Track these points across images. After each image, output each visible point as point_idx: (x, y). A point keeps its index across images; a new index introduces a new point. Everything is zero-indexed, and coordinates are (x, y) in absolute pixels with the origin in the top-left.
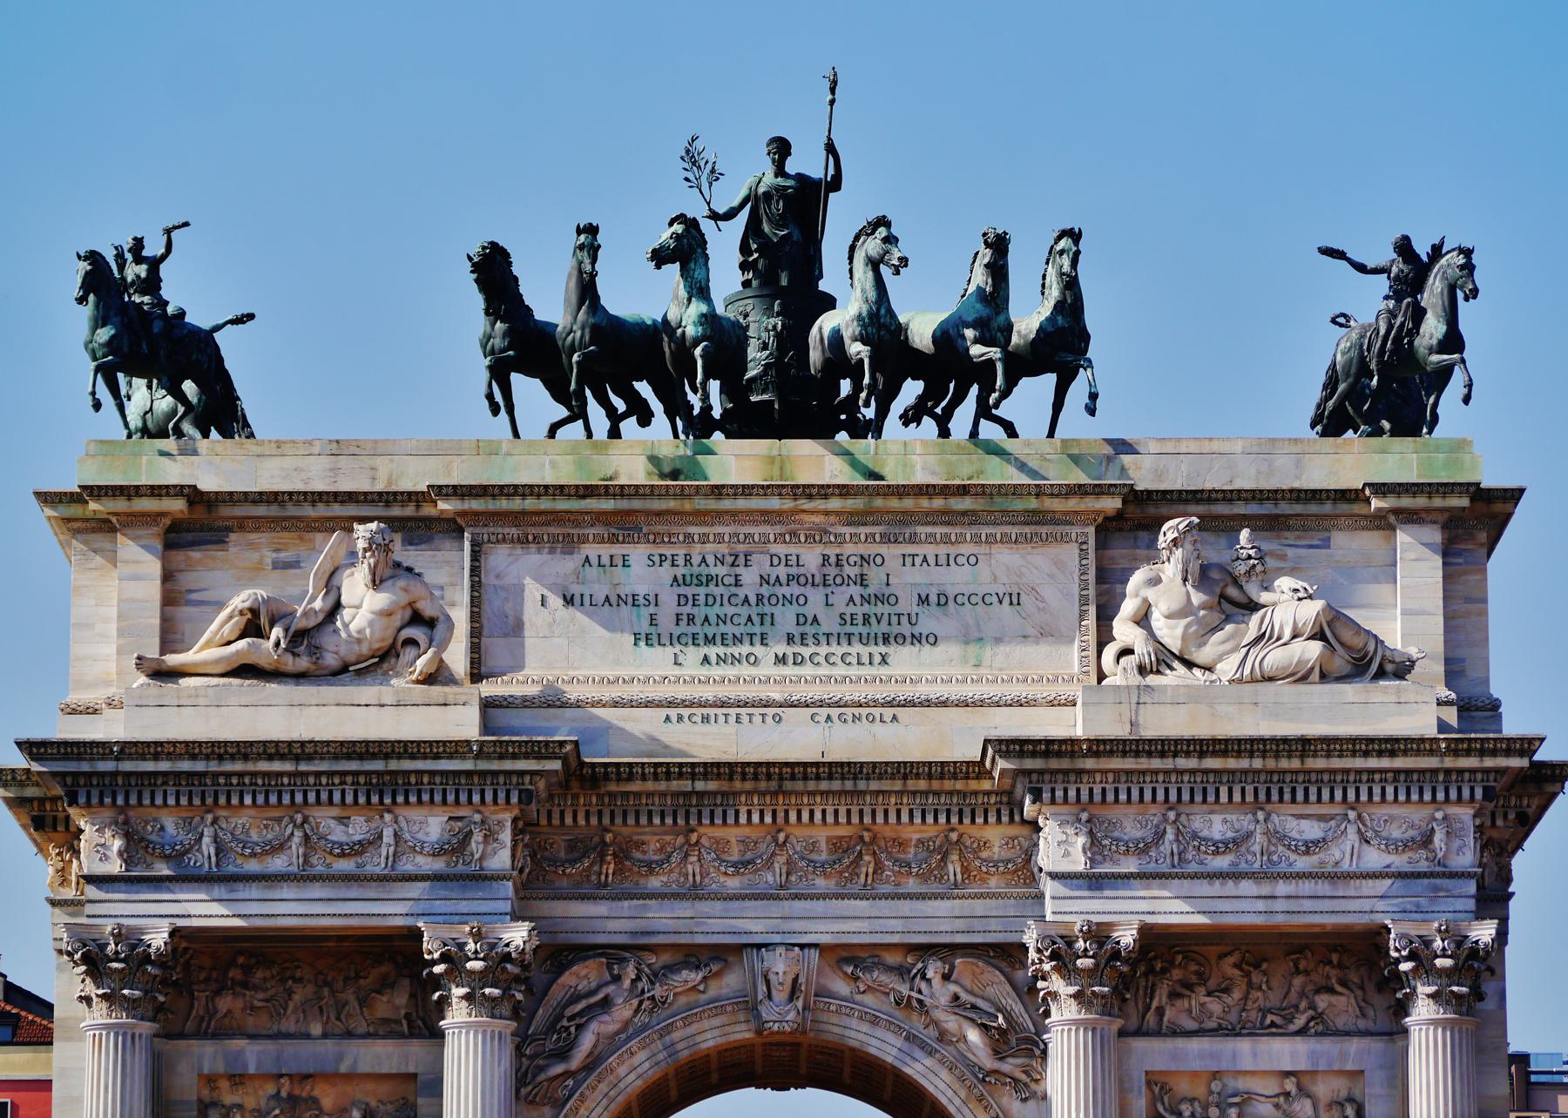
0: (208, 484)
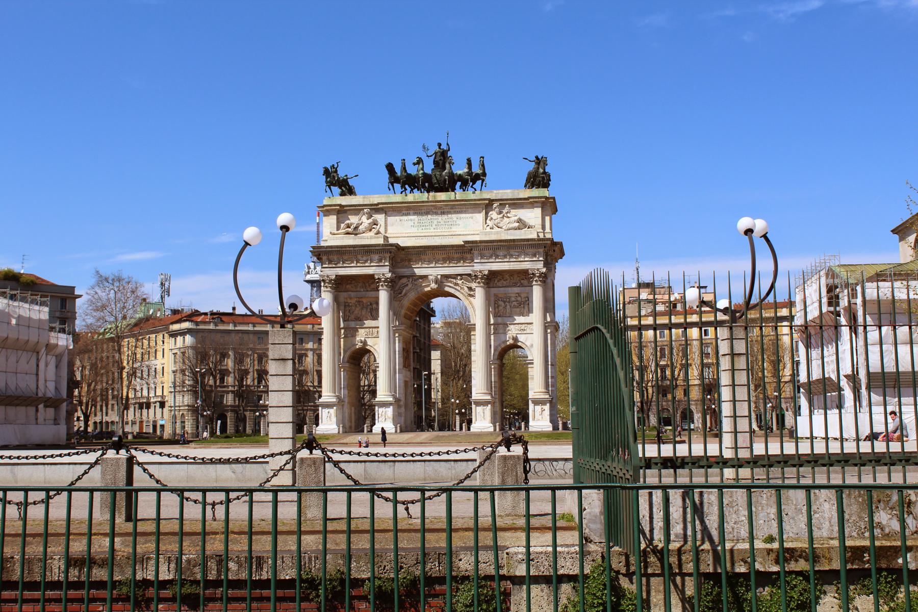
0: (344, 204)
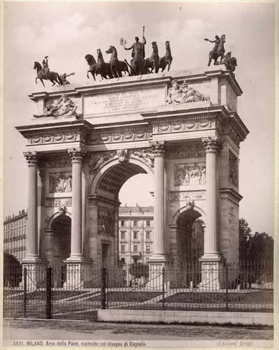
0: (48, 92)
